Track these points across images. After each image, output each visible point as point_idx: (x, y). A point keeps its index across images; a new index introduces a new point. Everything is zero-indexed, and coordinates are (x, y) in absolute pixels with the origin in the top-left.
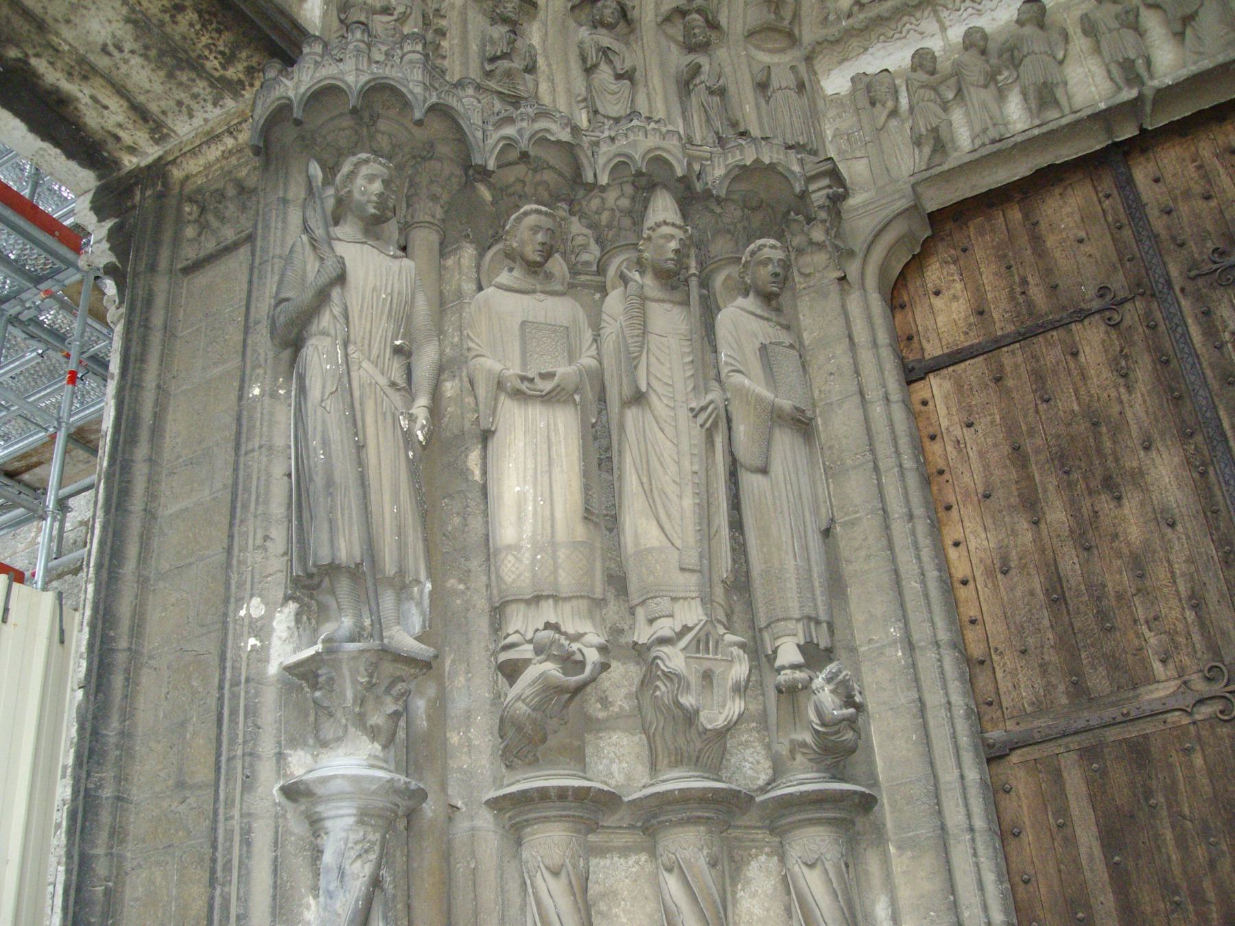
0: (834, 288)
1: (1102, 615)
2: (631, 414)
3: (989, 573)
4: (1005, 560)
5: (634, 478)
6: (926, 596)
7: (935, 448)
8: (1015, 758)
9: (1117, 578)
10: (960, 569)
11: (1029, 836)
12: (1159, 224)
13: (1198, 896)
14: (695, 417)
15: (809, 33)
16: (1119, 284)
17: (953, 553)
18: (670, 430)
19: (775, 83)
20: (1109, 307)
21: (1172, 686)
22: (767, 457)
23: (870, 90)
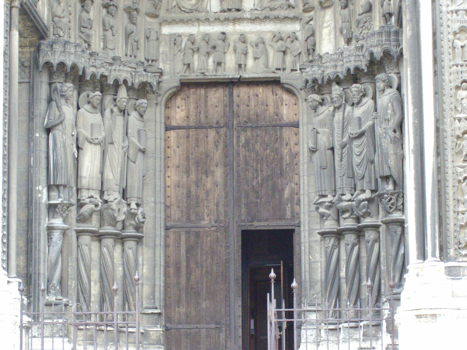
0: (154, 105)
1: (197, 203)
2: (110, 146)
3: (175, 186)
4: (179, 184)
5: (109, 162)
6: (160, 191)
7: (168, 150)
8: (172, 230)
9: (202, 195)
10: (168, 184)
11: (171, 247)
12: (235, 108)
13: (202, 266)
14: (123, 149)
15: (162, 13)
16: (222, 122)
17: (167, 179)
18: (117, 151)
19: (151, 38)
20: (218, 127)
21: (207, 222)
22: (136, 159)
23: (175, 40)
